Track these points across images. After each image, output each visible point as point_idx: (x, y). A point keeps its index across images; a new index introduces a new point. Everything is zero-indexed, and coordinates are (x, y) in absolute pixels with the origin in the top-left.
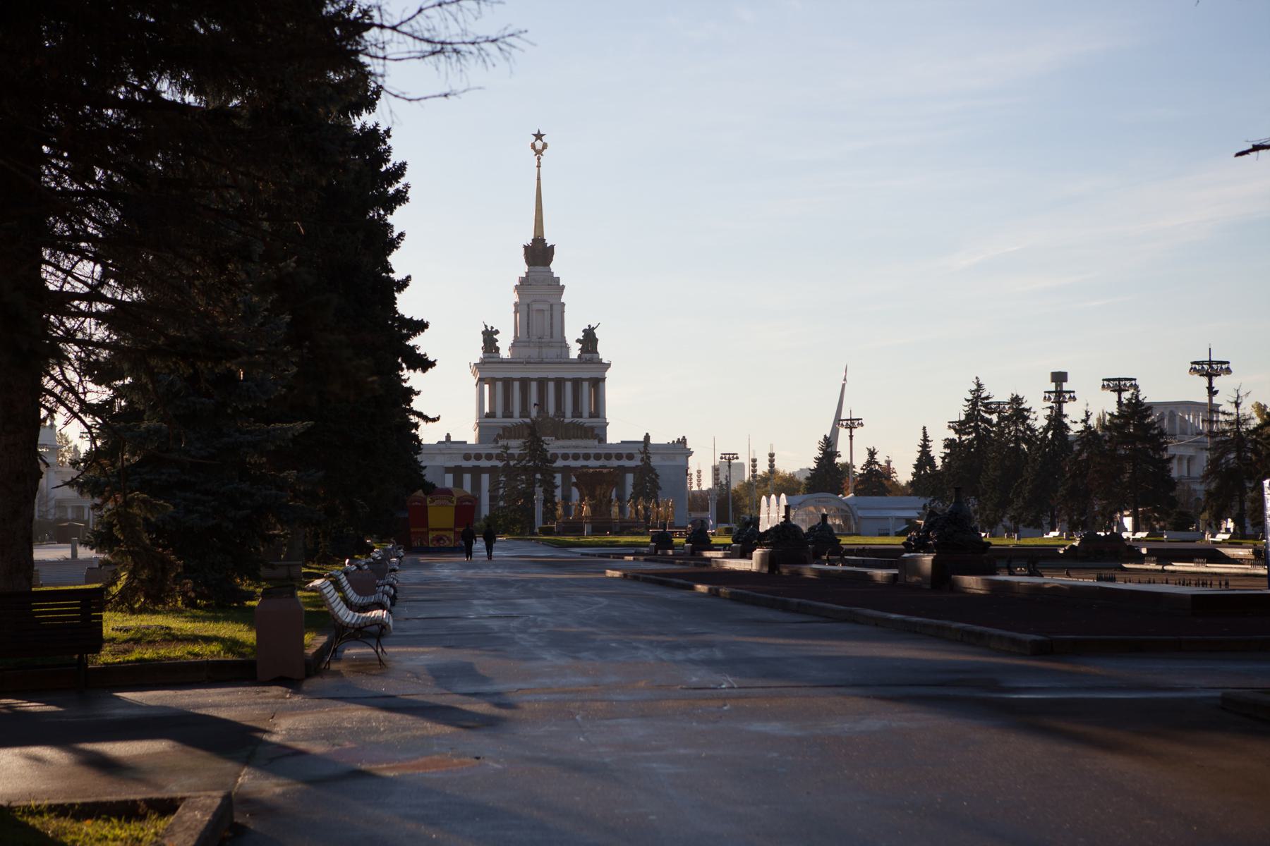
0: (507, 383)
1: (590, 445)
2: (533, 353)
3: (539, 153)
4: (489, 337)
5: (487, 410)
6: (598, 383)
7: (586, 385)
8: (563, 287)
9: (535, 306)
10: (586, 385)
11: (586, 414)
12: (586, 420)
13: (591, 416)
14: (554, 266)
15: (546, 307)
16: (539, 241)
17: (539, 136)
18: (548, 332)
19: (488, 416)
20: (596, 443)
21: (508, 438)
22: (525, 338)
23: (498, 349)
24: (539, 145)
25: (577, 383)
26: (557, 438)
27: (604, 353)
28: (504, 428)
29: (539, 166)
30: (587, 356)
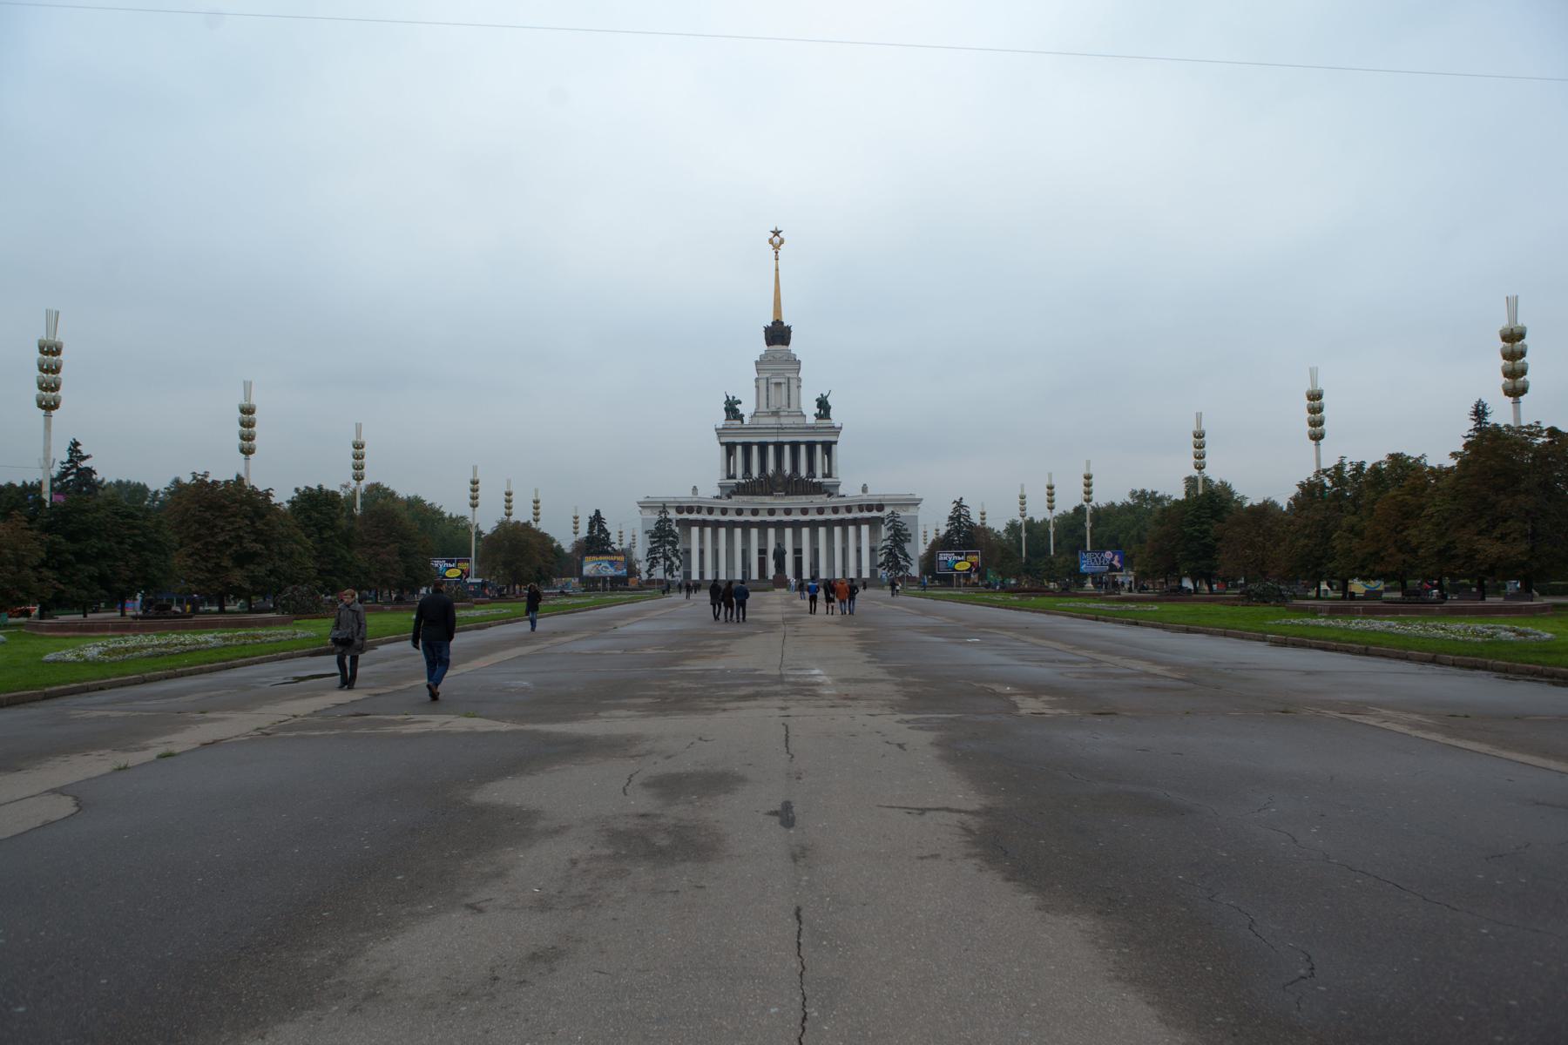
0: (747, 447)
1: (819, 500)
2: (772, 421)
3: (777, 248)
6: (828, 447)
7: (819, 448)
10: (819, 448)
11: (819, 473)
12: (819, 478)
13: (825, 476)
16: (778, 323)
17: (776, 233)
18: (785, 402)
20: (824, 497)
22: (763, 408)
24: (776, 240)
25: (811, 446)
27: (836, 417)
28: (738, 485)
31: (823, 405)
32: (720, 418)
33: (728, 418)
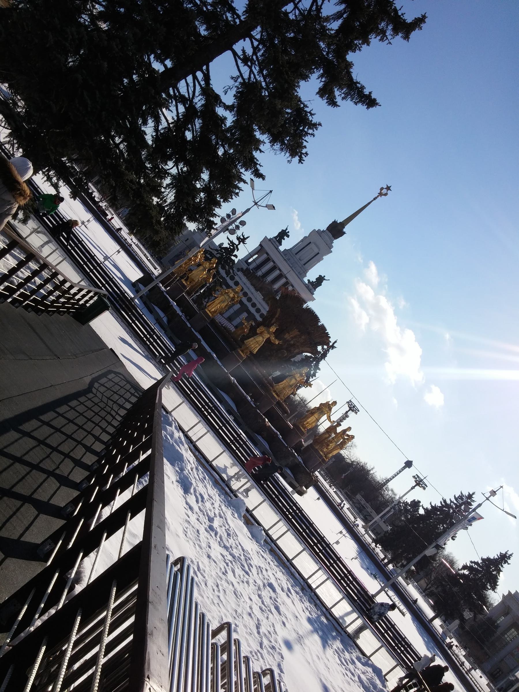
0: (268, 260)
3: (381, 194)
4: (283, 234)
5: (250, 261)
8: (331, 252)
9: (312, 246)
14: (335, 241)
15: (316, 251)
17: (388, 188)
19: (246, 262)
21: (245, 275)
23: (280, 244)
24: (384, 191)
26: (264, 299)
29: (375, 199)
30: (311, 286)
31: (320, 280)
32: (273, 234)
33: (276, 238)
